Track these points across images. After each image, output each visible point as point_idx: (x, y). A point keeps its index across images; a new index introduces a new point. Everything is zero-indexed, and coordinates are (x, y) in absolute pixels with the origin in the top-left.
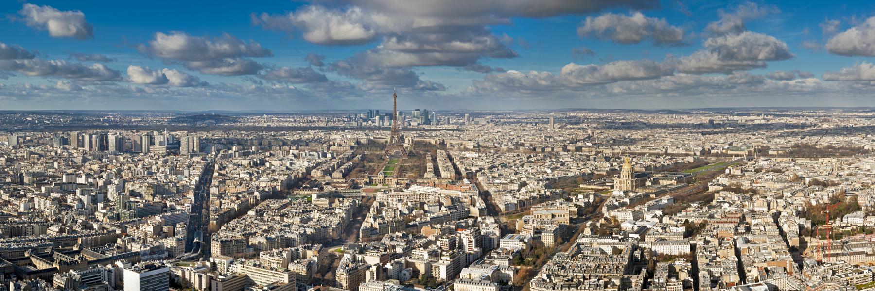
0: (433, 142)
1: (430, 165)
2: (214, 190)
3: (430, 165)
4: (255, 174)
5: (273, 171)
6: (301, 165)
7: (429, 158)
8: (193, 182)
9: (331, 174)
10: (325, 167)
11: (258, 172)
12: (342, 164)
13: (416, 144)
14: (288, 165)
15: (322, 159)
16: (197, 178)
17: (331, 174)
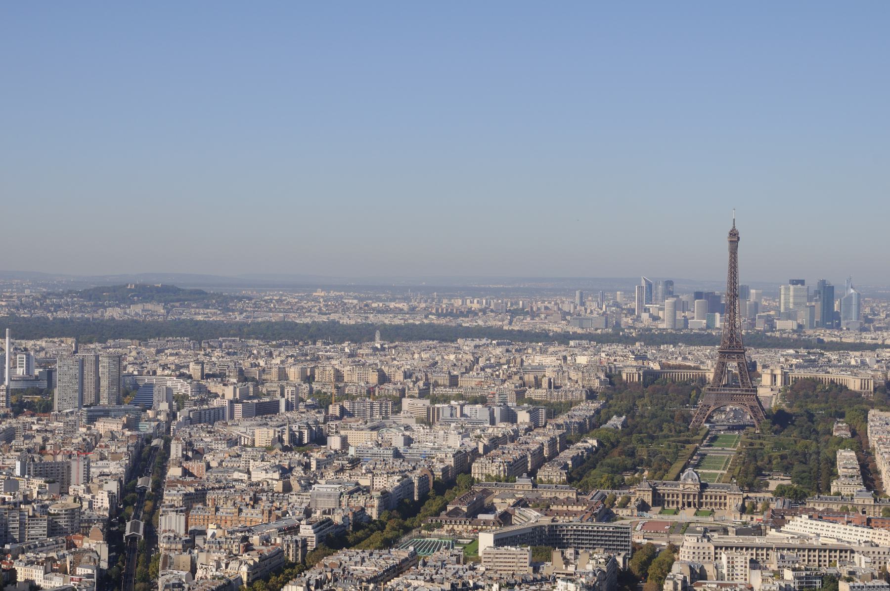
0: (854, 384)
1: (846, 458)
2: (171, 523)
3: (846, 458)
4: (299, 471)
5: (355, 463)
6: (443, 444)
7: (840, 430)
8: (103, 501)
9: (532, 474)
10: (513, 452)
11: (307, 467)
12: (566, 443)
13: (798, 389)
14: (398, 442)
15: (502, 428)
16: (113, 486)
17: (532, 474)
